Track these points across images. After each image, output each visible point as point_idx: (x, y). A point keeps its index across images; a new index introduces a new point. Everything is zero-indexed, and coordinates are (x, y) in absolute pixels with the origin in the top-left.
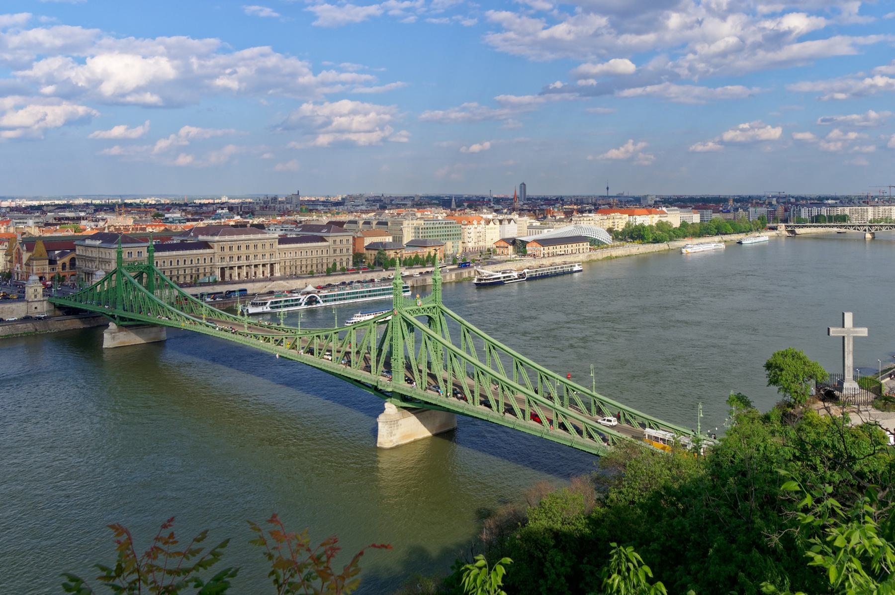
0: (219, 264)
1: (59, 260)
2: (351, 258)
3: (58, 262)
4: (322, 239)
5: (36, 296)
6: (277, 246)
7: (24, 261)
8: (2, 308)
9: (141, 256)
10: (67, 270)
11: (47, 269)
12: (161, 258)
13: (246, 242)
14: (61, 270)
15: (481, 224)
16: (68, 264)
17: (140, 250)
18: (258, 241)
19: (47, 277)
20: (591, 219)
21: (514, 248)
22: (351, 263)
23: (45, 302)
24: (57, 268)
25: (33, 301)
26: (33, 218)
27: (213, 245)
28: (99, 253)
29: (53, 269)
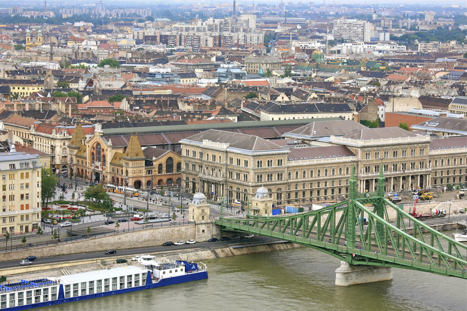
0: (363, 175)
1: (155, 161)
3: (154, 163)
5: (203, 217)
7: (109, 159)
9: (281, 165)
10: (164, 173)
12: (301, 168)
13: (394, 147)
14: (157, 173)
18: (407, 146)
19: (144, 181)
24: (153, 170)
25: (201, 224)
28: (227, 159)
29: (149, 171)
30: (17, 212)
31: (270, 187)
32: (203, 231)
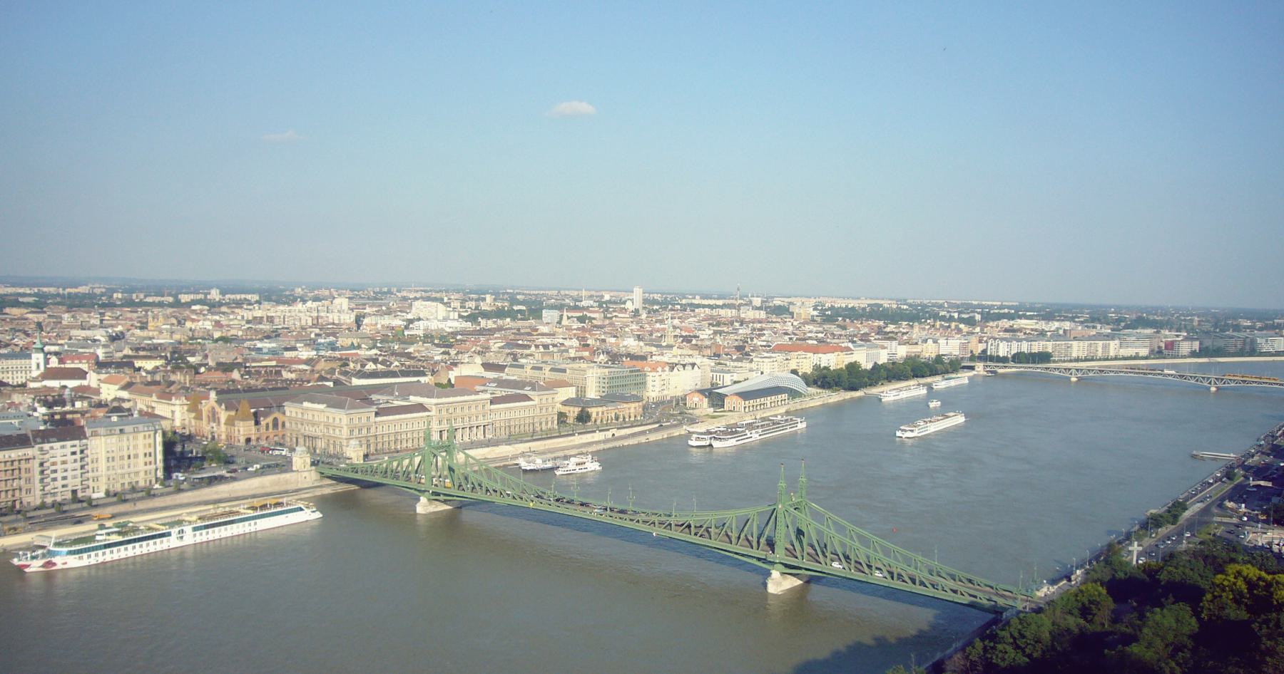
2: (556, 417)
3: (262, 423)
4: (527, 398)
5: (305, 466)
6: (488, 407)
7: (223, 420)
8: (279, 479)
10: (271, 430)
11: (253, 429)
15: (665, 371)
16: (271, 425)
17: (368, 415)
19: (253, 438)
20: (775, 360)
21: (709, 401)
22: (556, 422)
23: (313, 472)
26: (101, 347)
27: (431, 408)
30: (140, 468)
31: (361, 439)
32: (305, 478)
